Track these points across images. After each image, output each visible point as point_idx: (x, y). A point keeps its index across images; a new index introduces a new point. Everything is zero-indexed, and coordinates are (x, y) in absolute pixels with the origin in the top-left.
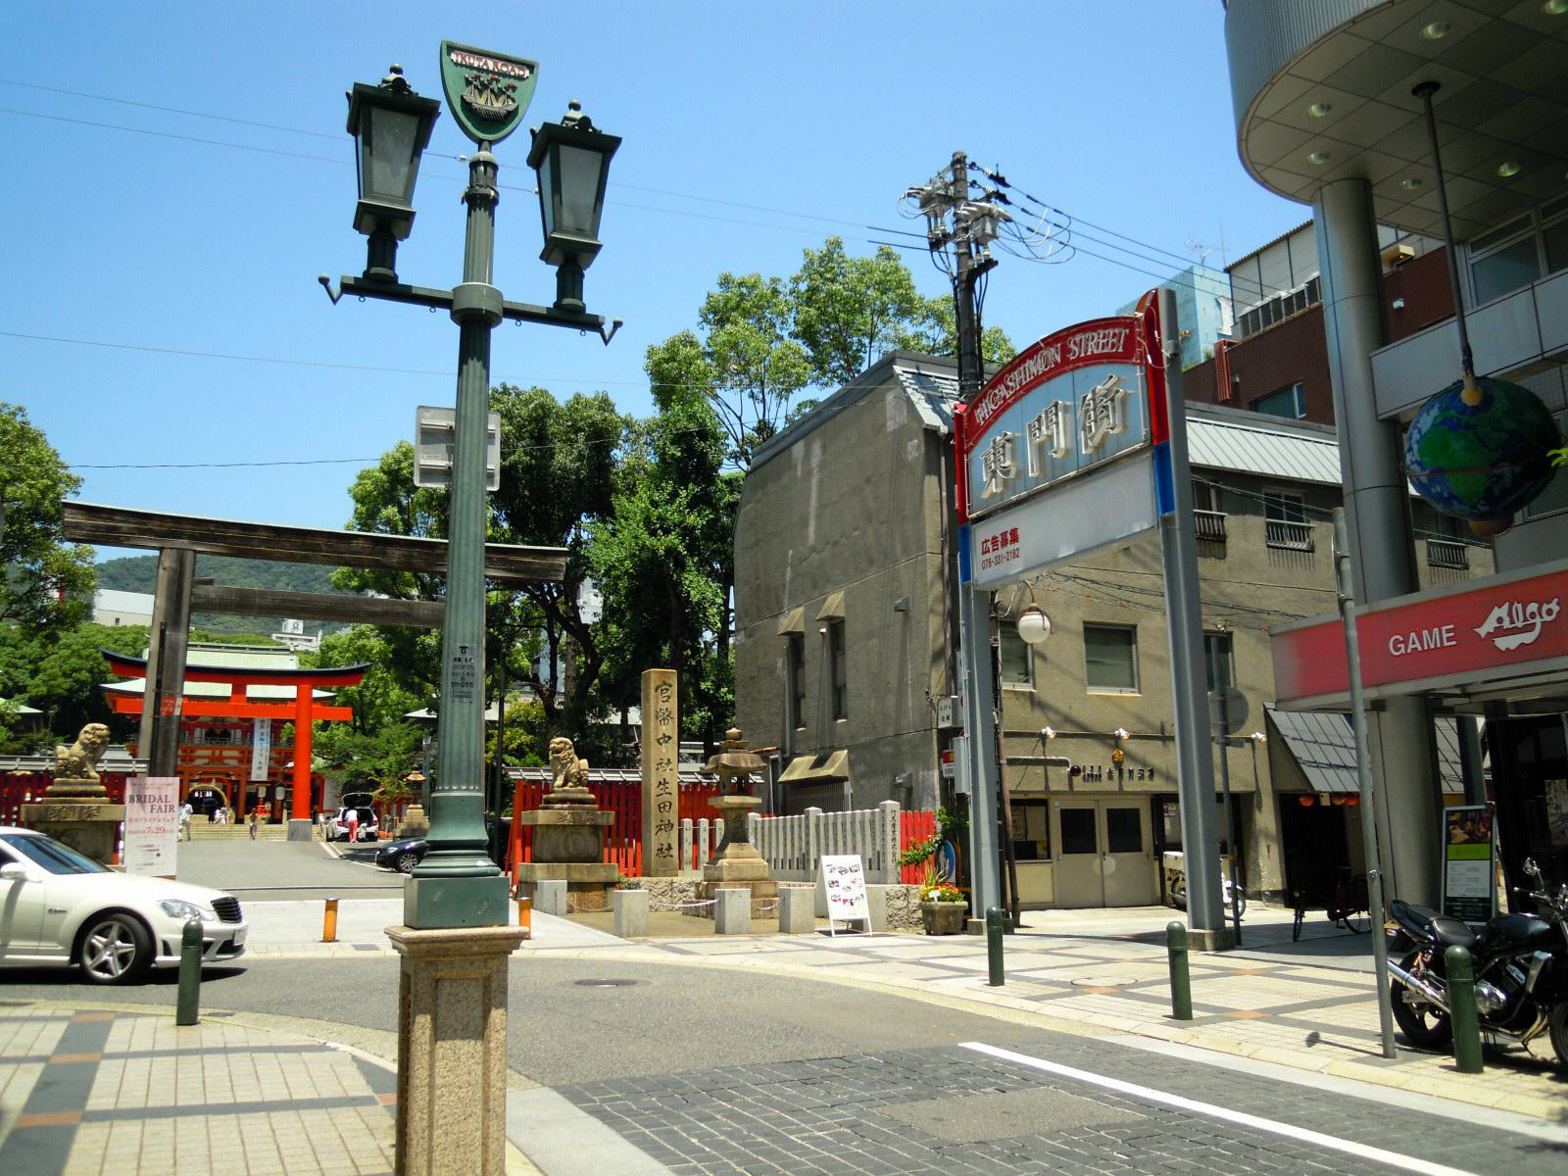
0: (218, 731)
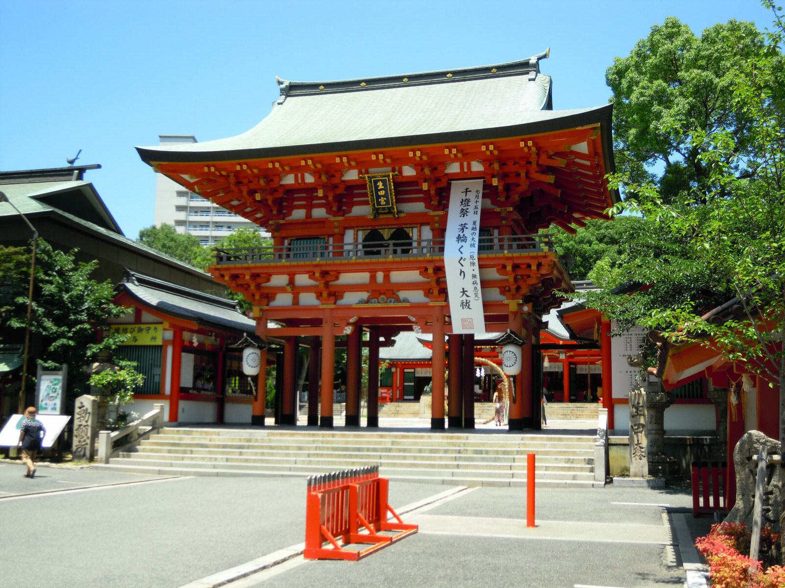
0: (386, 234)
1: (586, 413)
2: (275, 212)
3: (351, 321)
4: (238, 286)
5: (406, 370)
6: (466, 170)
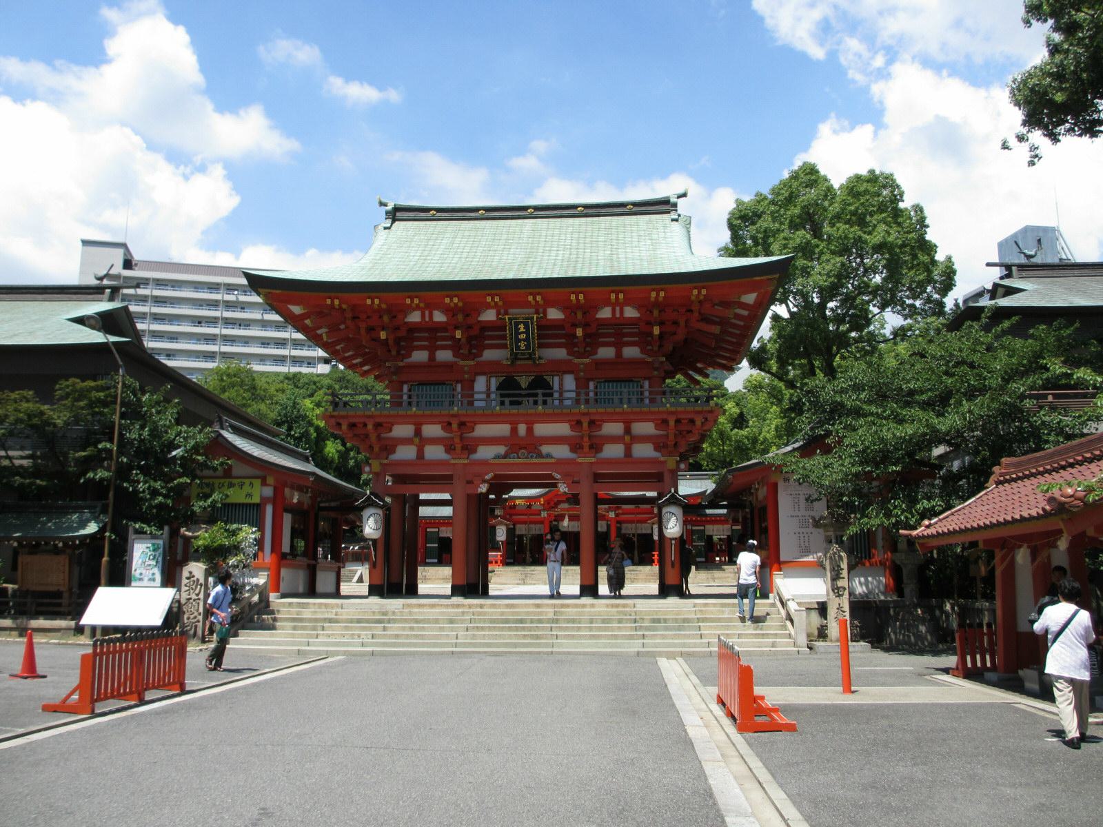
0: (524, 382)
1: (640, 576)
2: (394, 353)
3: (487, 477)
4: (355, 435)
5: (428, 530)
6: (618, 315)
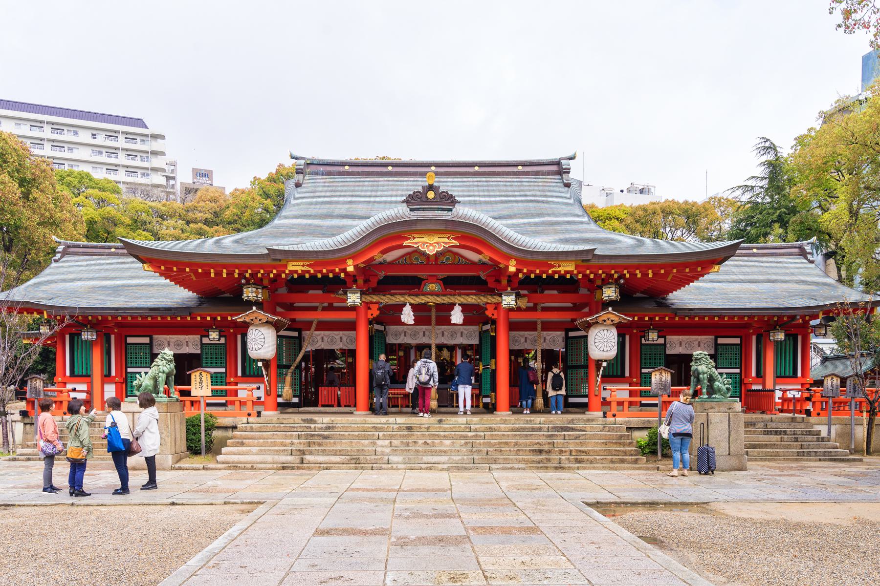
5: (130, 340)
